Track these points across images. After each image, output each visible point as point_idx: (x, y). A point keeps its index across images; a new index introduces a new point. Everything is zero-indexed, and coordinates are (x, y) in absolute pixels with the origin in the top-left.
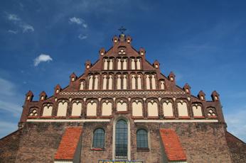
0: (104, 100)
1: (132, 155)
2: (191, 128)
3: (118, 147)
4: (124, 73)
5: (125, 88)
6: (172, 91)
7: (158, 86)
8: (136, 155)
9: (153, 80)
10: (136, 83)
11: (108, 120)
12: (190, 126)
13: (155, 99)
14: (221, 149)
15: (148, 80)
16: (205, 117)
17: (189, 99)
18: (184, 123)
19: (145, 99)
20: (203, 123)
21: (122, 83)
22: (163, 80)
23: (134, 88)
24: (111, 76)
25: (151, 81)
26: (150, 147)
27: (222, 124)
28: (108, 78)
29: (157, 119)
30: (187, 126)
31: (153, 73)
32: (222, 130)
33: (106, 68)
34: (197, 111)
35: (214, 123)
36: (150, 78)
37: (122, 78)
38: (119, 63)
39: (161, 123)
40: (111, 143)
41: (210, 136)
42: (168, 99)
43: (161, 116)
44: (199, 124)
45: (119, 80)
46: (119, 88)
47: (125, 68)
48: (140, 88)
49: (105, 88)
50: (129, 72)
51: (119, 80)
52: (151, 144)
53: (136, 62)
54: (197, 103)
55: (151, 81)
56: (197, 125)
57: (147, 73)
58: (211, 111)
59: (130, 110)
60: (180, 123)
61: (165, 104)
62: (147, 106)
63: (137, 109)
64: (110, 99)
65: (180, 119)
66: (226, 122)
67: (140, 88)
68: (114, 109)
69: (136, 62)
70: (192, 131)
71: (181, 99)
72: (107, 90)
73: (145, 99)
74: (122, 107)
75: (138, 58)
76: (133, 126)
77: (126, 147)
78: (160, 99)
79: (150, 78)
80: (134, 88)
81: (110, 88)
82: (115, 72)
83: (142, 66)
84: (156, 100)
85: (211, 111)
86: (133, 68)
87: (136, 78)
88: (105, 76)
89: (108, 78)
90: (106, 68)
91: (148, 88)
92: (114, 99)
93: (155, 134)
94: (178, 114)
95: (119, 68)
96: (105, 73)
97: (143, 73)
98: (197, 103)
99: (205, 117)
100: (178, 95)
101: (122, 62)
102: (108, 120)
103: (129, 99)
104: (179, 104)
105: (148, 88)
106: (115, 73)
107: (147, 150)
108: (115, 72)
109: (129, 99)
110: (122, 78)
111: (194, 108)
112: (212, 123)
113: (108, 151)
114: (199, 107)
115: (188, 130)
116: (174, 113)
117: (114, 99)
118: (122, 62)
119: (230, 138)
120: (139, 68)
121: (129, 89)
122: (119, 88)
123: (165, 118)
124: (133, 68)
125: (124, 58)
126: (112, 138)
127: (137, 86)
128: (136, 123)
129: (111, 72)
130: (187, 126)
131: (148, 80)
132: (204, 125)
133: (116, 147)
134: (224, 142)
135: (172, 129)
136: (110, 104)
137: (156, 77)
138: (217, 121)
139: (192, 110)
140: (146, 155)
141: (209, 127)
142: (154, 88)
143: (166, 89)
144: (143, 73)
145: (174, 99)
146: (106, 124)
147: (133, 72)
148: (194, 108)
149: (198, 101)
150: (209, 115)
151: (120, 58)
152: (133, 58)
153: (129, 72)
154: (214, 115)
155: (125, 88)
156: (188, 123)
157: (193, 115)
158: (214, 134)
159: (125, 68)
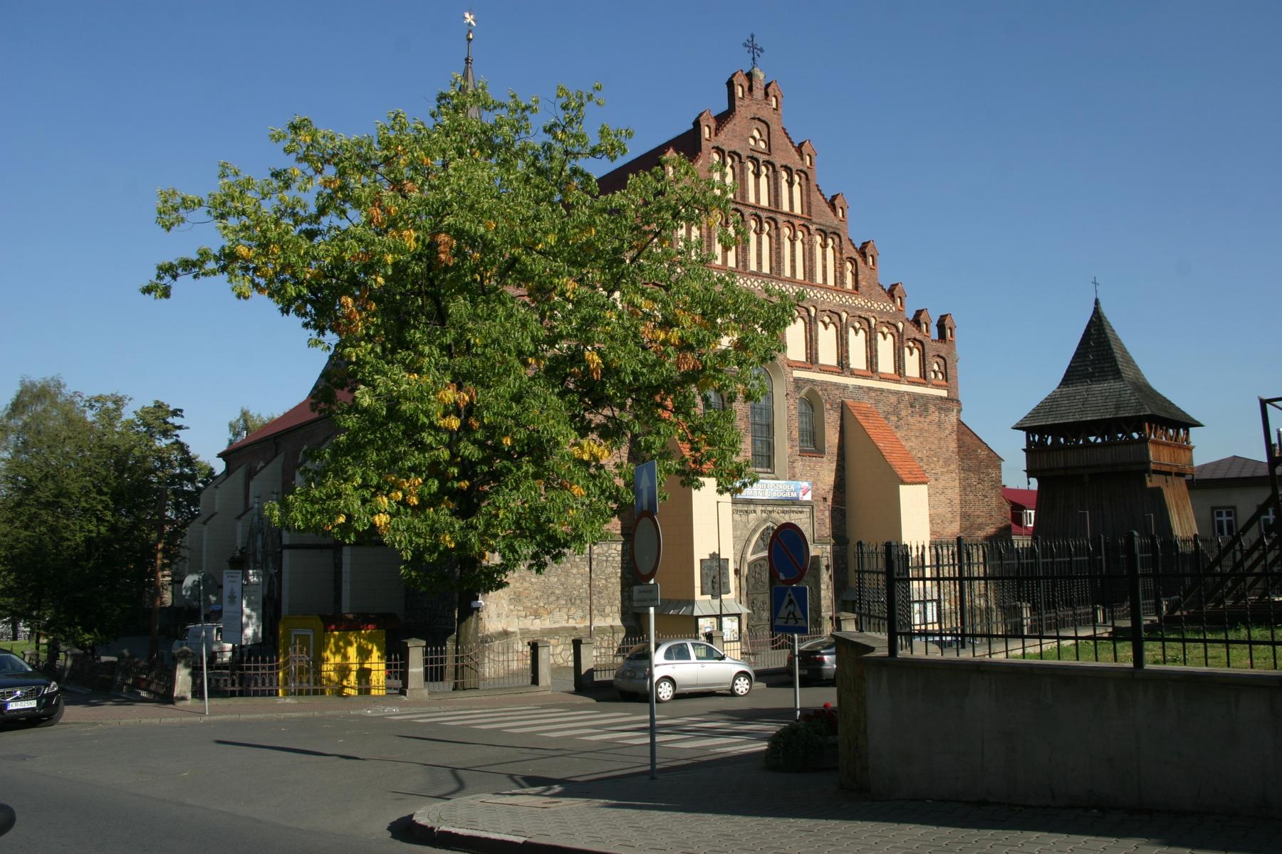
6: (870, 298)
14: (947, 462)
17: (900, 325)
18: (889, 391)
20: (922, 396)
29: (832, 372)
39: (846, 387)
44: (915, 398)
48: (800, 275)
60: (882, 391)
70: (903, 413)
76: (791, 387)
100: (881, 312)
119: (968, 440)
128: (797, 380)
130: (893, 399)
134: (953, 446)
137: (839, 250)
138: (944, 393)
141: (932, 408)
156: (897, 393)
158: (939, 424)
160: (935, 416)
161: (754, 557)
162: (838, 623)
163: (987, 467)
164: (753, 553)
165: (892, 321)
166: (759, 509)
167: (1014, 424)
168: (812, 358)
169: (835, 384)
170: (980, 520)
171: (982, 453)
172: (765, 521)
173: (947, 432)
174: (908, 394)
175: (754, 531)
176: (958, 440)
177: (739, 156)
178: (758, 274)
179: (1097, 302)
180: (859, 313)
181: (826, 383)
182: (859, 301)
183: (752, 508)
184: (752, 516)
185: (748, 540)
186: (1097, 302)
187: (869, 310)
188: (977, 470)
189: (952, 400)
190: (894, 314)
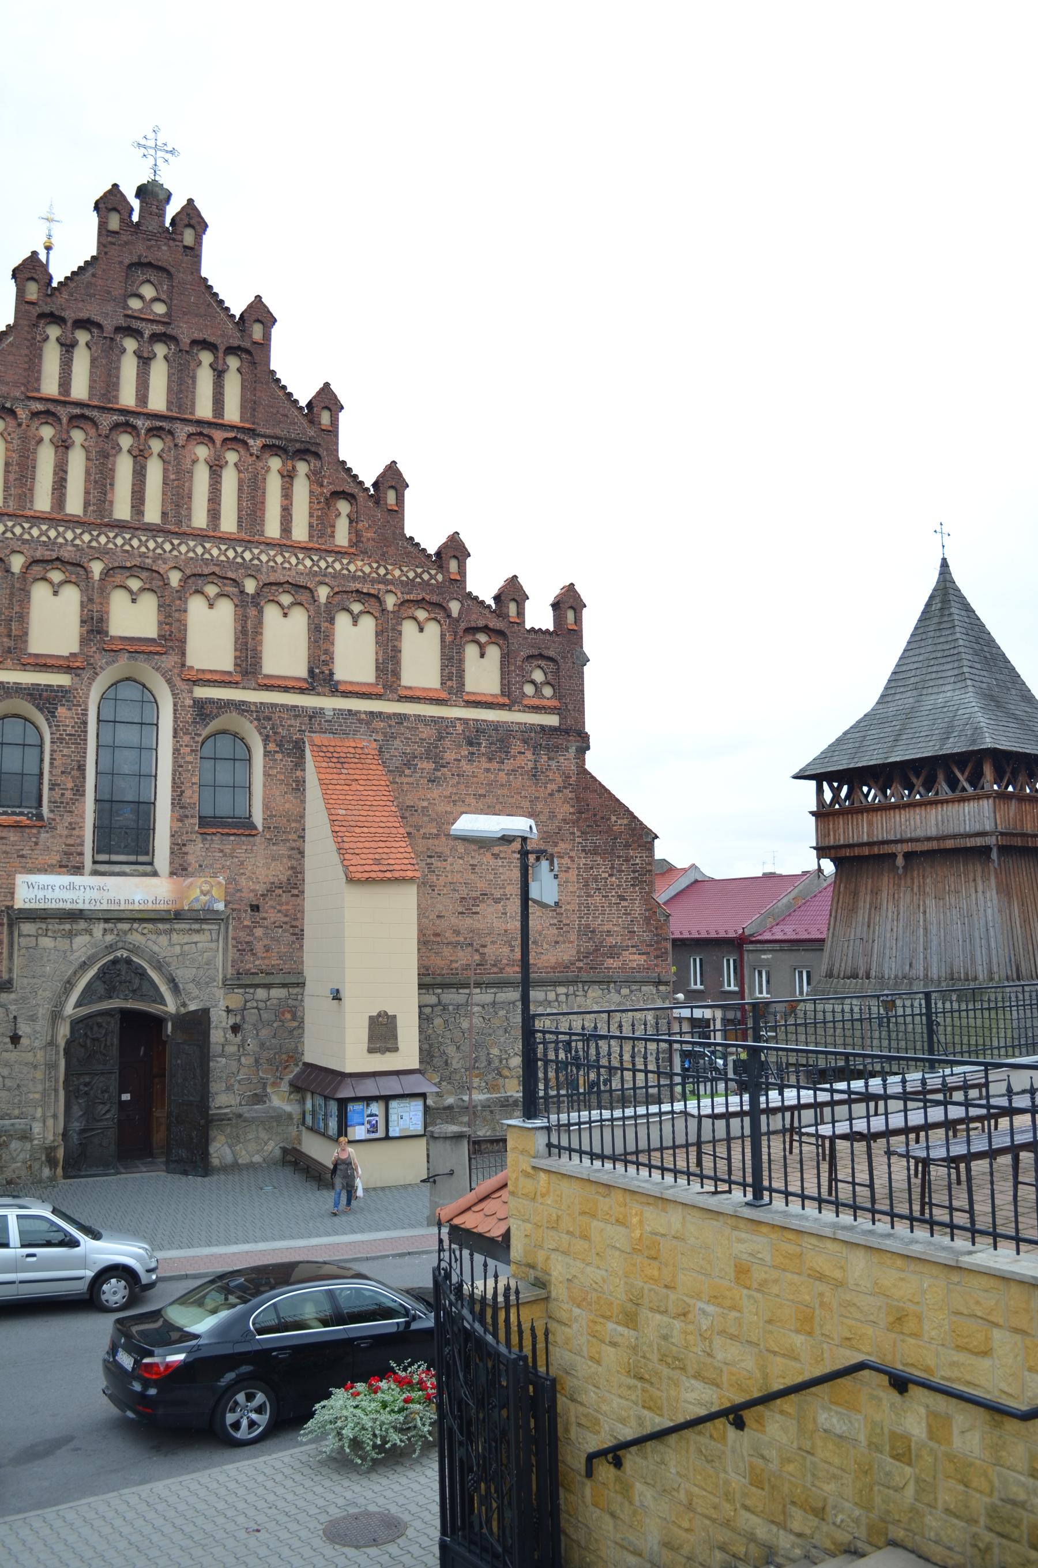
0: (37, 569)
1: (178, 849)
2: (447, 743)
3: (106, 805)
4: (155, 432)
5: (152, 514)
6: (383, 558)
7: (322, 526)
8: (196, 850)
9: (301, 489)
10: (216, 494)
11: (61, 680)
12: (440, 738)
13: (301, 590)
15: (274, 485)
16: (509, 698)
17: (455, 607)
18: (418, 717)
19: (250, 586)
20: (496, 726)
21: (138, 487)
22: (350, 497)
23: (200, 519)
24: (78, 436)
25: (287, 494)
26: (258, 819)
27: (573, 735)
28: (63, 446)
29: (302, 691)
30: (427, 733)
31: (306, 452)
32: (567, 761)
33: (50, 387)
34: (483, 672)
35: (543, 728)
36: (288, 477)
37: (140, 457)
38: (129, 367)
39: (316, 714)
40: (79, 791)
41: (518, 782)
42: (361, 596)
43: (320, 677)
45: (124, 467)
46: (122, 511)
47: (158, 401)
48: (229, 524)
49: (43, 502)
50: (182, 431)
51: (124, 467)
52: (266, 807)
53: (219, 374)
54: (486, 629)
55: (287, 494)
56: (475, 735)
57: (272, 449)
58: (538, 676)
59: (172, 638)
60: (402, 718)
61: (343, 620)
62: (259, 622)
63: (210, 632)
64: (74, 568)
65: (402, 699)
66: (588, 728)
67: (229, 524)
68: (94, 625)
69: (219, 374)
70: (450, 756)
71: (420, 603)
72: (58, 518)
73: (250, 586)
74: (133, 617)
75: (231, 350)
77: (145, 809)
78: (323, 593)
79: (288, 477)
80: (200, 519)
81: (74, 505)
82: (106, 421)
83: (248, 405)
84: (304, 597)
85: (538, 676)
86: (204, 410)
87: (216, 469)
88: (47, 432)
89: (63, 446)
90: (50, 387)
91: (272, 529)
92: (97, 568)
93: (289, 761)
94: (397, 674)
95: (127, 398)
96: (48, 416)
97: (256, 444)
98: (486, 629)
99: (509, 698)
101: (145, 361)
102: (61, 680)
103: (175, 578)
104: (408, 628)
105: (272, 529)
106: (100, 420)
107: (244, 826)
108: (106, 421)
109: (175, 578)
110: (140, 457)
111: (471, 651)
112: (532, 728)
113: (61, 830)
114: (494, 653)
115: (433, 753)
116: (381, 669)
117: (97, 568)
118: (145, 361)
119: (594, 800)
120: (232, 414)
121: (175, 524)
122: (122, 511)
123: (335, 689)
124: (204, 410)
125: (156, 338)
126: (82, 768)
127: (214, 514)
129: (81, 416)
131: (274, 485)
132: (501, 739)
133: (99, 813)
135: (368, 743)
136: (71, 596)
137: (315, 478)
138: (553, 720)
139: (461, 661)
140: (240, 852)
141: (517, 746)
142: (300, 533)
143: (357, 547)
144: (256, 444)
145: (390, 601)
146: (46, 699)
147: (202, 430)
148: (471, 651)
149: (494, 623)
150: (529, 690)
151: (136, 333)
152: (209, 346)
153: (182, 431)
154: (548, 691)
155: (152, 514)
156: (436, 721)
157: (462, 684)
158: (534, 775)
159: (158, 401)
160: (527, 760)
161: (84, 1011)
162: (725, 1065)
163: (627, 846)
164: (79, 1004)
165: (435, 599)
166: (98, 929)
167: (796, 770)
168: (248, 663)
169: (294, 707)
170: (612, 940)
171: (619, 823)
172: (111, 948)
173: (551, 787)
174: (465, 721)
175: (84, 966)
176: (577, 798)
177: (99, 326)
178: (136, 527)
179: (945, 564)
180: (358, 586)
181: (274, 705)
182: (359, 566)
183: (82, 925)
184: (80, 941)
185: (69, 985)
186: (945, 564)
187: (383, 580)
188: (609, 853)
189: (567, 732)
190: (439, 586)
